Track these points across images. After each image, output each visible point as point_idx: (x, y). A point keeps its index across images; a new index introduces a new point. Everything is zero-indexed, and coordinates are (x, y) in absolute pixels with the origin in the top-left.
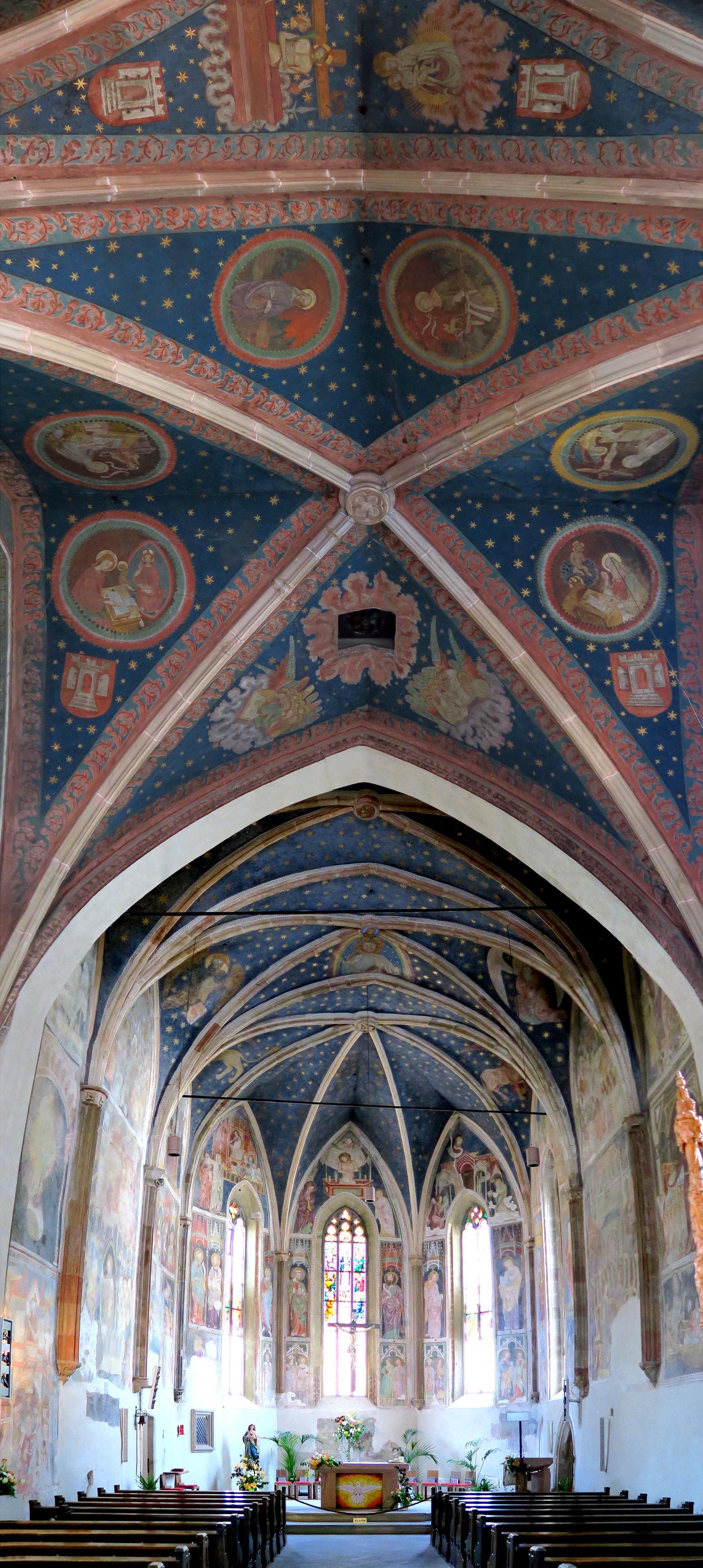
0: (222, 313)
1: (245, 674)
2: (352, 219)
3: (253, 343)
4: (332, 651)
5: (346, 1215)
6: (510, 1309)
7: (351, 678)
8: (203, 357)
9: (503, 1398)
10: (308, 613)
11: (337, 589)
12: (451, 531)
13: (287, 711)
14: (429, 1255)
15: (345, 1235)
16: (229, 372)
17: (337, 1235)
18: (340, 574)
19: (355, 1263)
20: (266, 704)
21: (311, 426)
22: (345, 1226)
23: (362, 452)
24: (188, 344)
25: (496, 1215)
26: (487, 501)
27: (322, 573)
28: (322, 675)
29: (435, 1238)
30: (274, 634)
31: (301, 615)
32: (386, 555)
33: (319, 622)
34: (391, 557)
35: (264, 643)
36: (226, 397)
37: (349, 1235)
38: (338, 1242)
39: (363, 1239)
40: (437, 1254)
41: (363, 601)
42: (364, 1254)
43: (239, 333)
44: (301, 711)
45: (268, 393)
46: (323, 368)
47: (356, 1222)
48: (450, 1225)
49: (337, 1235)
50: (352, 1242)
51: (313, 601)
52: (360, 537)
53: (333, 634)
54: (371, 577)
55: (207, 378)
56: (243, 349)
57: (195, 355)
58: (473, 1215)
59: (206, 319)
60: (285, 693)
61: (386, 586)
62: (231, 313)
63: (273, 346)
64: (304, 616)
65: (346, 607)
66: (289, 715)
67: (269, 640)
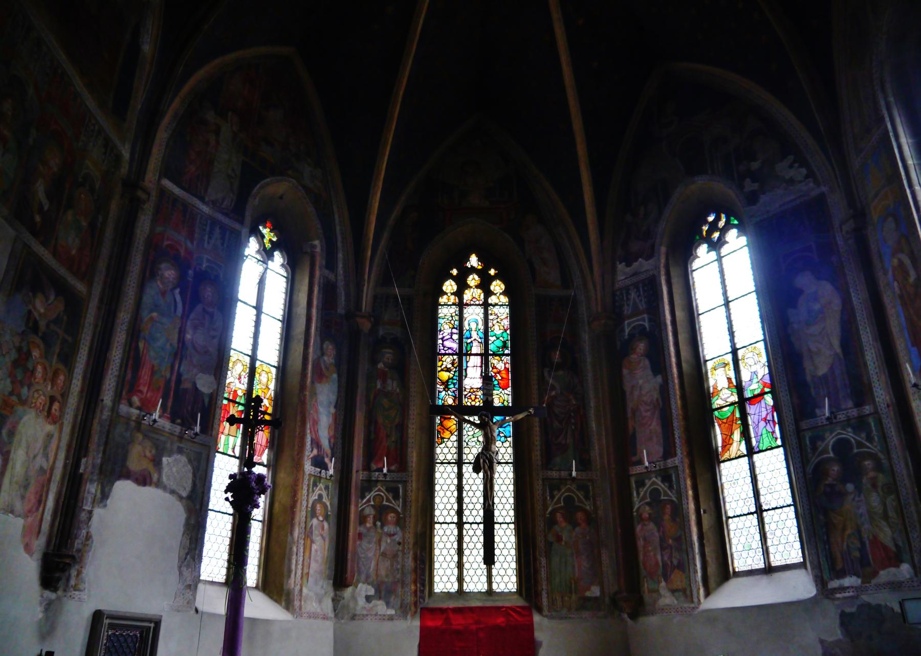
5: (474, 261)
6: (823, 370)
9: (841, 574)
14: (627, 310)
15: (473, 294)
17: (459, 294)
19: (492, 339)
22: (473, 280)
25: (763, 199)
29: (635, 279)
37: (479, 293)
38: (461, 305)
39: (504, 300)
40: (642, 306)
42: (506, 323)
47: (492, 272)
48: (663, 249)
49: (459, 294)
50: (486, 305)
58: (705, 228)
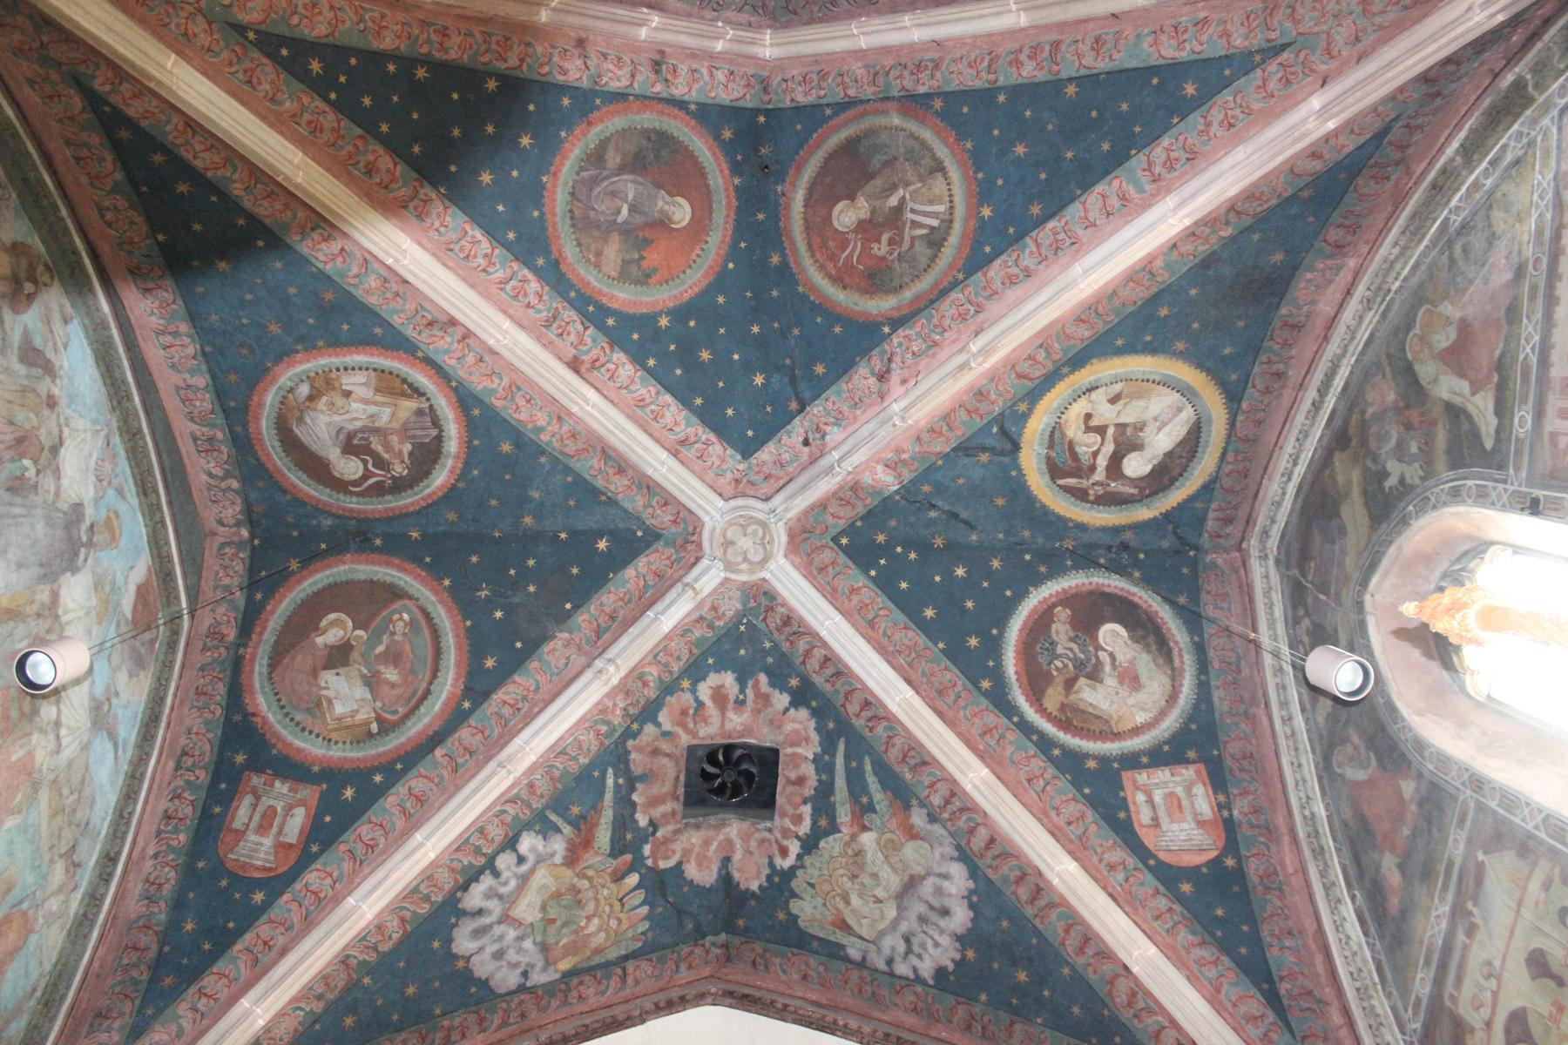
0: (558, 210)
1: (527, 826)
2: (749, 103)
3: (597, 266)
4: (674, 813)
7: (702, 874)
8: (526, 272)
10: (640, 731)
11: (687, 697)
12: (869, 594)
13: (589, 918)
16: (558, 303)
18: (695, 671)
20: (557, 895)
21: (668, 414)
23: (741, 467)
24: (507, 245)
26: (924, 547)
27: (666, 665)
28: (654, 853)
30: (584, 760)
31: (629, 734)
32: (768, 645)
33: (656, 752)
34: (776, 646)
35: (565, 773)
36: (551, 343)
41: (729, 726)
43: (579, 245)
44: (613, 923)
45: (612, 350)
46: (692, 323)
51: (649, 713)
52: (731, 607)
53: (677, 778)
54: (742, 682)
55: (528, 305)
56: (582, 272)
57: (515, 266)
59: (536, 214)
60: (590, 879)
61: (765, 699)
62: (571, 211)
63: (624, 276)
64: (634, 735)
65: (702, 733)
66: (592, 928)
67: (574, 768)
